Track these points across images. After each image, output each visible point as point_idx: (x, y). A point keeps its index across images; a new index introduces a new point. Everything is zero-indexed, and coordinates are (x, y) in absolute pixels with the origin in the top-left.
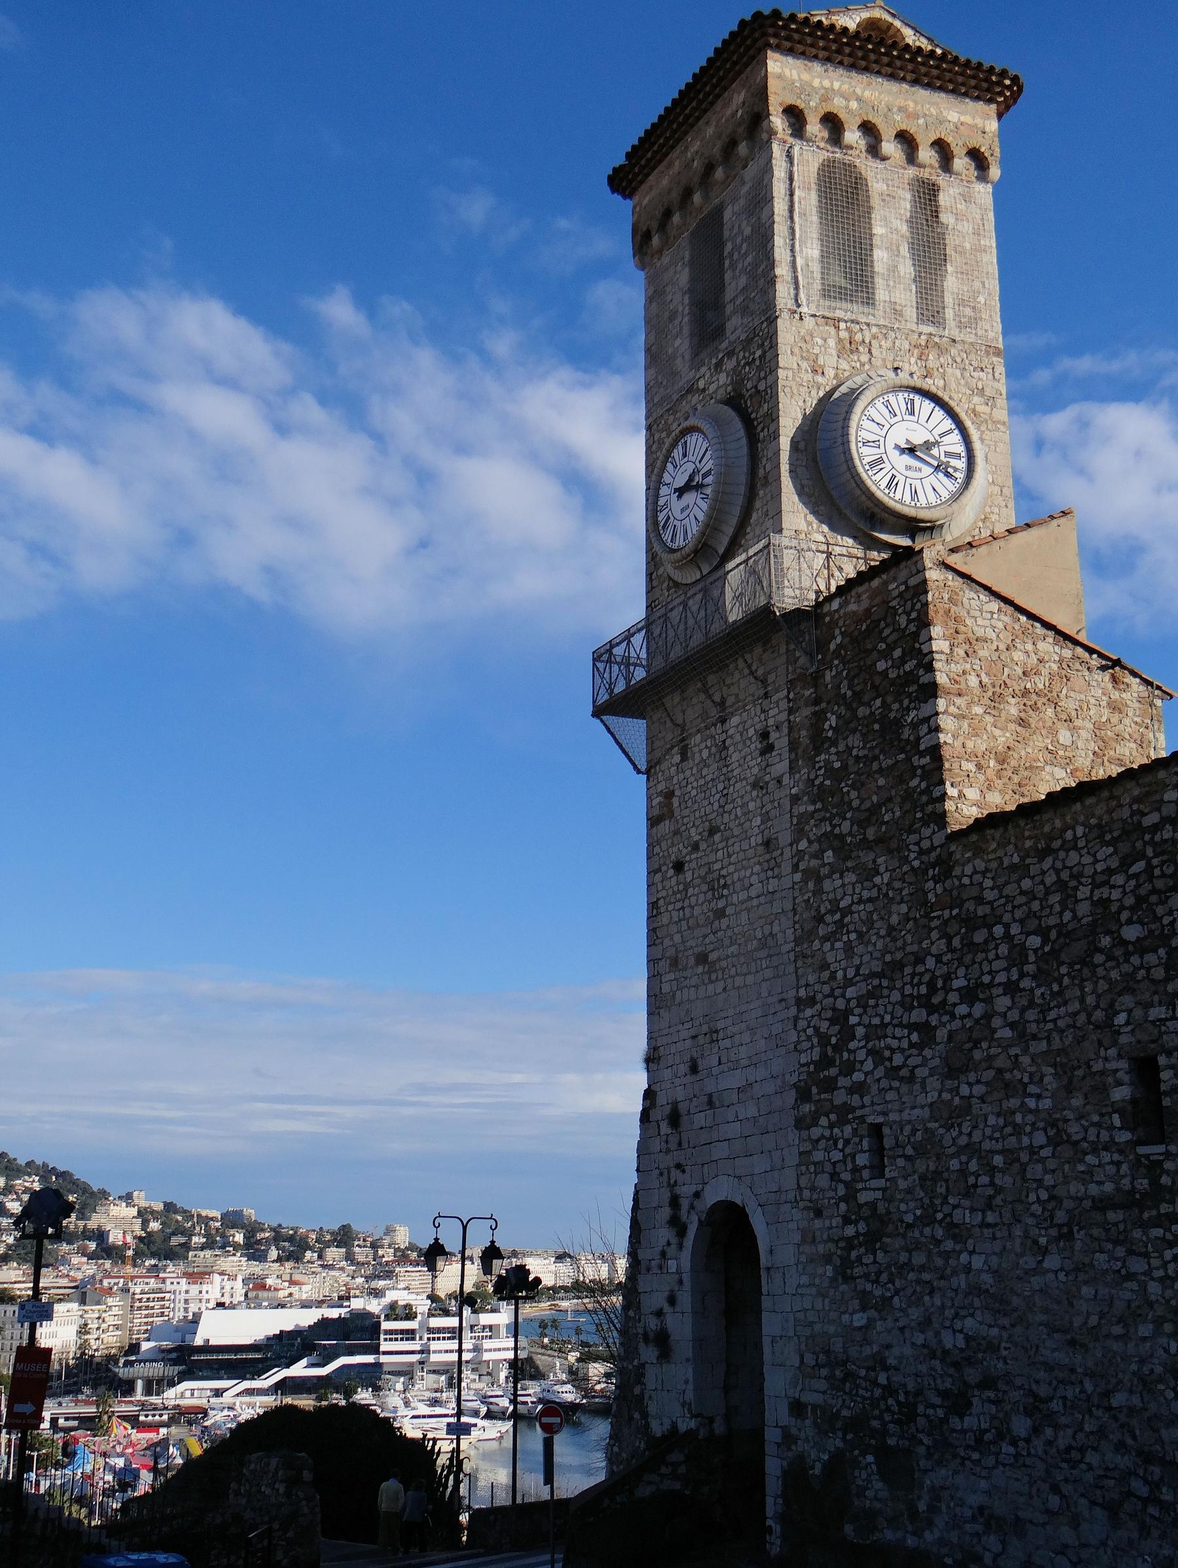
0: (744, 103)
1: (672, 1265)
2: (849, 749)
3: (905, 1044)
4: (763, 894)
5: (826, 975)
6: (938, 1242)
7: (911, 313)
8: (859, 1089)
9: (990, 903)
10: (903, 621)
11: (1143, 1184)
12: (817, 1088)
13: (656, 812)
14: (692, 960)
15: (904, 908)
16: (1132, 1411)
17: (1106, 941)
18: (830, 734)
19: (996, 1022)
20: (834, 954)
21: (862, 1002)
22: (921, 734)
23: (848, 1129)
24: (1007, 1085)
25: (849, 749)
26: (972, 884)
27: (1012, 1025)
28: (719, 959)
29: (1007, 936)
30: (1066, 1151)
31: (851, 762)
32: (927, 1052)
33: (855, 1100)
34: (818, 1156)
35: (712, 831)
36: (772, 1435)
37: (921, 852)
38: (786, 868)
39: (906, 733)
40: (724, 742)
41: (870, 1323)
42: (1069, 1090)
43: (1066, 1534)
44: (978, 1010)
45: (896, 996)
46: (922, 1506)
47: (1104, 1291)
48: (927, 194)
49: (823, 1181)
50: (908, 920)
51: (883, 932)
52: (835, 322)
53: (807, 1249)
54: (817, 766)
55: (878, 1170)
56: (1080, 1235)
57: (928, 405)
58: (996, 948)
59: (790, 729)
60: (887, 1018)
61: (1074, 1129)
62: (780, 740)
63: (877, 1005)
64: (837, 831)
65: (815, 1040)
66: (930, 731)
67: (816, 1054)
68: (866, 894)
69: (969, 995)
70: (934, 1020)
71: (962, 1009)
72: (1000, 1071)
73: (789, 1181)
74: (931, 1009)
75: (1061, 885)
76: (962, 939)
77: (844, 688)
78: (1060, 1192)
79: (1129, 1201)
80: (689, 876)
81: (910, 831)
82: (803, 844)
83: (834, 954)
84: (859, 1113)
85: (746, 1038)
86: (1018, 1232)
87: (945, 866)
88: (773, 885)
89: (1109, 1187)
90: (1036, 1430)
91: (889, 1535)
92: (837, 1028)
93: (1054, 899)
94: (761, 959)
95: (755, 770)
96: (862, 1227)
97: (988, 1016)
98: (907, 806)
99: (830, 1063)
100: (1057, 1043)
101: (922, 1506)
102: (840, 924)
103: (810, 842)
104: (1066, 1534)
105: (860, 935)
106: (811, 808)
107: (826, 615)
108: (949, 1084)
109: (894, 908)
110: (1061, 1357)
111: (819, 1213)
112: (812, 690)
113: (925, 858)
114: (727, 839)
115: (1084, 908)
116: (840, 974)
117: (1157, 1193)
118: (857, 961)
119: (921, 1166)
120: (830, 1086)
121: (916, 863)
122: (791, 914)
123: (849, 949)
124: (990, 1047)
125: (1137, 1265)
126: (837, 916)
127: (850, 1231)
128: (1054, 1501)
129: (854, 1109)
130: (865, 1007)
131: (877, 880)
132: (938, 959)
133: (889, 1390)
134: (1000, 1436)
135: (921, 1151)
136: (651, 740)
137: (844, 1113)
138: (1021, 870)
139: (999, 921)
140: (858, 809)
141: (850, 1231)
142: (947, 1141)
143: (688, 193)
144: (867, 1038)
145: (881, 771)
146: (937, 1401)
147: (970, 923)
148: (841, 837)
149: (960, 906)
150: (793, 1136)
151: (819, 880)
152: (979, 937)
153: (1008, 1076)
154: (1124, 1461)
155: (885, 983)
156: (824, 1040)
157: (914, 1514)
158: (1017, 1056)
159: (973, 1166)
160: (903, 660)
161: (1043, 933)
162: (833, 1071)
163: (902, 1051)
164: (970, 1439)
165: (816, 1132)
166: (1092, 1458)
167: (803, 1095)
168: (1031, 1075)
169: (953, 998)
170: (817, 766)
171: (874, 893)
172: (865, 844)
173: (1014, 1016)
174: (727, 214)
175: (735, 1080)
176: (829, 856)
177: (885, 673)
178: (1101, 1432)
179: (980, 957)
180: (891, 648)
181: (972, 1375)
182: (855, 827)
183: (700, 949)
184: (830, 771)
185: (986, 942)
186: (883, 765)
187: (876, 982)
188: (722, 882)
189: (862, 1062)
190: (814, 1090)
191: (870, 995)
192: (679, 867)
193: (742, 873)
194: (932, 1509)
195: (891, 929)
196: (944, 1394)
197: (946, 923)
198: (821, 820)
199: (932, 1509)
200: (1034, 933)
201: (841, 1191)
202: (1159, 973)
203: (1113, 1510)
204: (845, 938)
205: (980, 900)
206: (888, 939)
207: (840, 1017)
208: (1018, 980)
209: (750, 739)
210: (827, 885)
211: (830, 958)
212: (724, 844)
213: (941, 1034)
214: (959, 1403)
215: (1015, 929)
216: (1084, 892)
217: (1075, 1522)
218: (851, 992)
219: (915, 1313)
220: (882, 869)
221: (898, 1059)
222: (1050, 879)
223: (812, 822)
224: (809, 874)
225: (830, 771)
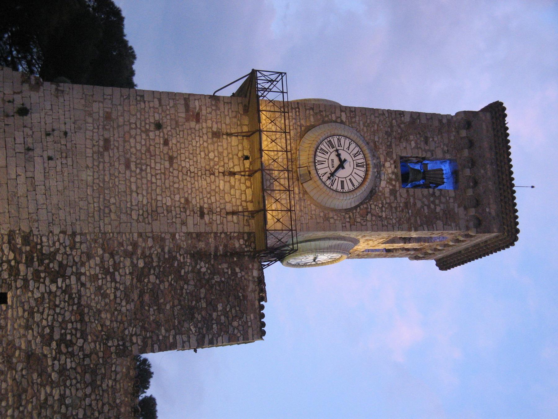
0: (490, 213)
2: (187, 282)
3: (44, 323)
4: (132, 205)
5: (84, 259)
9: (101, 386)
10: (235, 324)
14: (106, 136)
15: (108, 323)
18: (198, 267)
21: (67, 290)
22: (183, 336)
24: (20, 396)
25: (187, 282)
26: (112, 371)
27: (46, 399)
28: (104, 162)
31: (182, 283)
32: (39, 339)
33: (20, 283)
35: (171, 159)
37: (132, 335)
39: (186, 325)
40: (214, 174)
44: (54, 376)
50: (102, 326)
51: (99, 307)
54: (185, 255)
58: (82, 389)
59: (207, 233)
60: (58, 310)
63: (65, 302)
64: (152, 272)
65: (52, 249)
66: (184, 342)
68: (118, 294)
69: (62, 371)
70: (54, 345)
71: (57, 368)
72: (26, 391)
76: (89, 365)
77: (217, 278)
81: (143, 328)
82: (150, 242)
84: (13, 284)
87: (123, 352)
92: (57, 268)
94: (99, 202)
95: (194, 202)
98: (154, 325)
102: (106, 272)
103: (152, 247)
105: (100, 288)
106: (166, 250)
107: (253, 266)
108: (23, 354)
109: (109, 316)
112: (221, 253)
113: (129, 337)
114: (164, 174)
116: (83, 270)
118: (88, 285)
120: (29, 263)
121: (127, 332)
122: (118, 230)
123: (94, 278)
124: (38, 384)
126: (111, 270)
129: (16, 282)
130: (64, 292)
131: (124, 303)
132: (81, 348)
139: (93, 391)
140: (159, 288)
144: (50, 292)
145: (173, 307)
147: (94, 373)
148: (149, 274)
149: (103, 364)
153: (24, 397)
155: (75, 308)
156: (52, 256)
158: (32, 402)
162: (36, 264)
163: (41, 320)
168: (23, 412)
170: (185, 255)
171: (118, 300)
175: (39, 177)
177: (215, 309)
179: (79, 377)
180: (226, 314)
182: (150, 286)
183: (112, 143)
184: (182, 265)
185: (85, 382)
186: (175, 308)
187: (76, 301)
188: (144, 167)
189: (38, 288)
190: (28, 248)
191: (70, 297)
192: (159, 126)
193: (144, 187)
195: (99, 312)
197: (97, 354)
198: (159, 258)
200: (85, 414)
204: (100, 276)
205: (104, 377)
206: (95, 310)
207: (61, 273)
208: (65, 404)
209: (210, 198)
211: (92, 262)
212: (163, 171)
215: (88, 401)
218: (73, 278)
220: (128, 307)
221: (37, 317)
223: (159, 250)
224: (135, 245)
225: (182, 265)
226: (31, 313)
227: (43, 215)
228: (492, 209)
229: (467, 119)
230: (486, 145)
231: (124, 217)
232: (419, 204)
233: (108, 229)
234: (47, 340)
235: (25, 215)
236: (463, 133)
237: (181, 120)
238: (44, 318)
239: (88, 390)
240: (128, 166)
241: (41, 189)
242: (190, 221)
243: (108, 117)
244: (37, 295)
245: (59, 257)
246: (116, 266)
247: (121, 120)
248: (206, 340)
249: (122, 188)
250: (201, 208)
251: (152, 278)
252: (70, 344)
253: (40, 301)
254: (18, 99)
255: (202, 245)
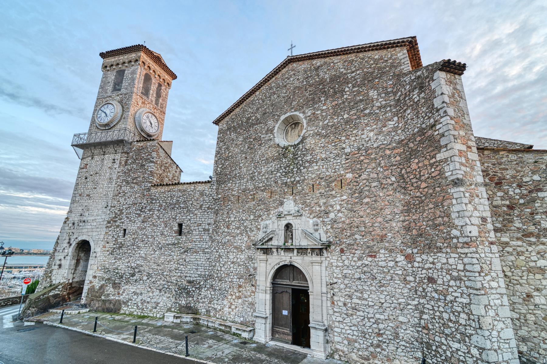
1: (66, 251)
6: (134, 249)
7: (154, 102)
8: (123, 223)
11: (176, 242)
12: (111, 222)
13: (82, 167)
16: (167, 275)
17: (177, 206)
19: (154, 215)
20: (122, 200)
23: (118, 229)
25: (133, 167)
29: (159, 202)
30: (163, 236)
33: (121, 224)
34: (110, 233)
36: (87, 282)
38: (114, 183)
39: (146, 167)
41: (116, 262)
42: (166, 227)
43: (151, 294)
44: (151, 213)
45: (134, 208)
46: (121, 292)
47: (166, 257)
48: (160, 85)
49: (110, 237)
52: (142, 98)
53: (104, 249)
55: (124, 236)
56: (163, 249)
57: (154, 117)
61: (166, 233)
62: (118, 162)
67: (114, 216)
69: (150, 210)
70: (142, 213)
73: (102, 237)
74: (141, 211)
75: (171, 196)
78: (161, 242)
79: (174, 244)
80: (88, 180)
82: (119, 180)
83: (122, 200)
85: (97, 211)
86: (151, 248)
87: (149, 190)
88: (110, 185)
89: (170, 242)
90: (148, 279)
91: (112, 297)
93: (169, 198)
96: (118, 246)
97: (153, 214)
99: (117, 218)
100: (165, 220)
101: (121, 292)
102: (124, 195)
104: (151, 294)
110: (156, 267)
111: (108, 243)
115: (174, 201)
117: (178, 243)
119: (133, 236)
120: (115, 221)
123: (125, 199)
125: (173, 254)
127: (115, 246)
128: (149, 290)
133: (118, 273)
134: (141, 280)
135: (134, 234)
136: (84, 154)
137: (118, 226)
138: (164, 193)
139: (158, 200)
141: (115, 246)
142: (140, 233)
143: (118, 64)
146: (128, 274)
147: (152, 199)
150: (105, 229)
151: (121, 187)
152: (154, 202)
154: (164, 283)
157: (119, 294)
159: (145, 237)
160: (148, 156)
161: (166, 203)
164: (134, 280)
165: (110, 229)
166: (158, 282)
167: (109, 222)
169: (146, 210)
172: (133, 183)
173: (158, 215)
174: (126, 72)
175: (93, 218)
176: (124, 183)
178: (161, 278)
180: (145, 153)
181: (137, 270)
184: (128, 169)
191: (129, 207)
194: (123, 292)
195: (135, 198)
196: (130, 274)
199: (123, 292)
201: (114, 239)
202: (185, 212)
203: (160, 290)
207: (121, 211)
210: (123, 188)
213: (143, 216)
214: (133, 275)
215: (161, 202)
216: (175, 198)
217: (153, 292)
219: (127, 260)
221: (132, 219)
222: (169, 195)
224: (118, 185)
226: (130, 221)
227: (103, 217)
228: (133, 56)
229: (105, 67)
230: (113, 60)
231: (110, 189)
232: (127, 84)
233: (112, 195)
234: (140, 215)
235: (102, 223)
236: (108, 68)
237: (86, 170)
238: (133, 216)
239: (158, 201)
240: (95, 188)
241: (96, 218)
242: (115, 166)
243: (80, 195)
244: (126, 219)
245: (116, 211)
246: (124, 192)
247: (82, 191)
248: (152, 160)
249: (101, 190)
250: (113, 163)
251: (129, 179)
252: (142, 208)
253: (128, 218)
254: (71, 225)
255: (123, 163)
